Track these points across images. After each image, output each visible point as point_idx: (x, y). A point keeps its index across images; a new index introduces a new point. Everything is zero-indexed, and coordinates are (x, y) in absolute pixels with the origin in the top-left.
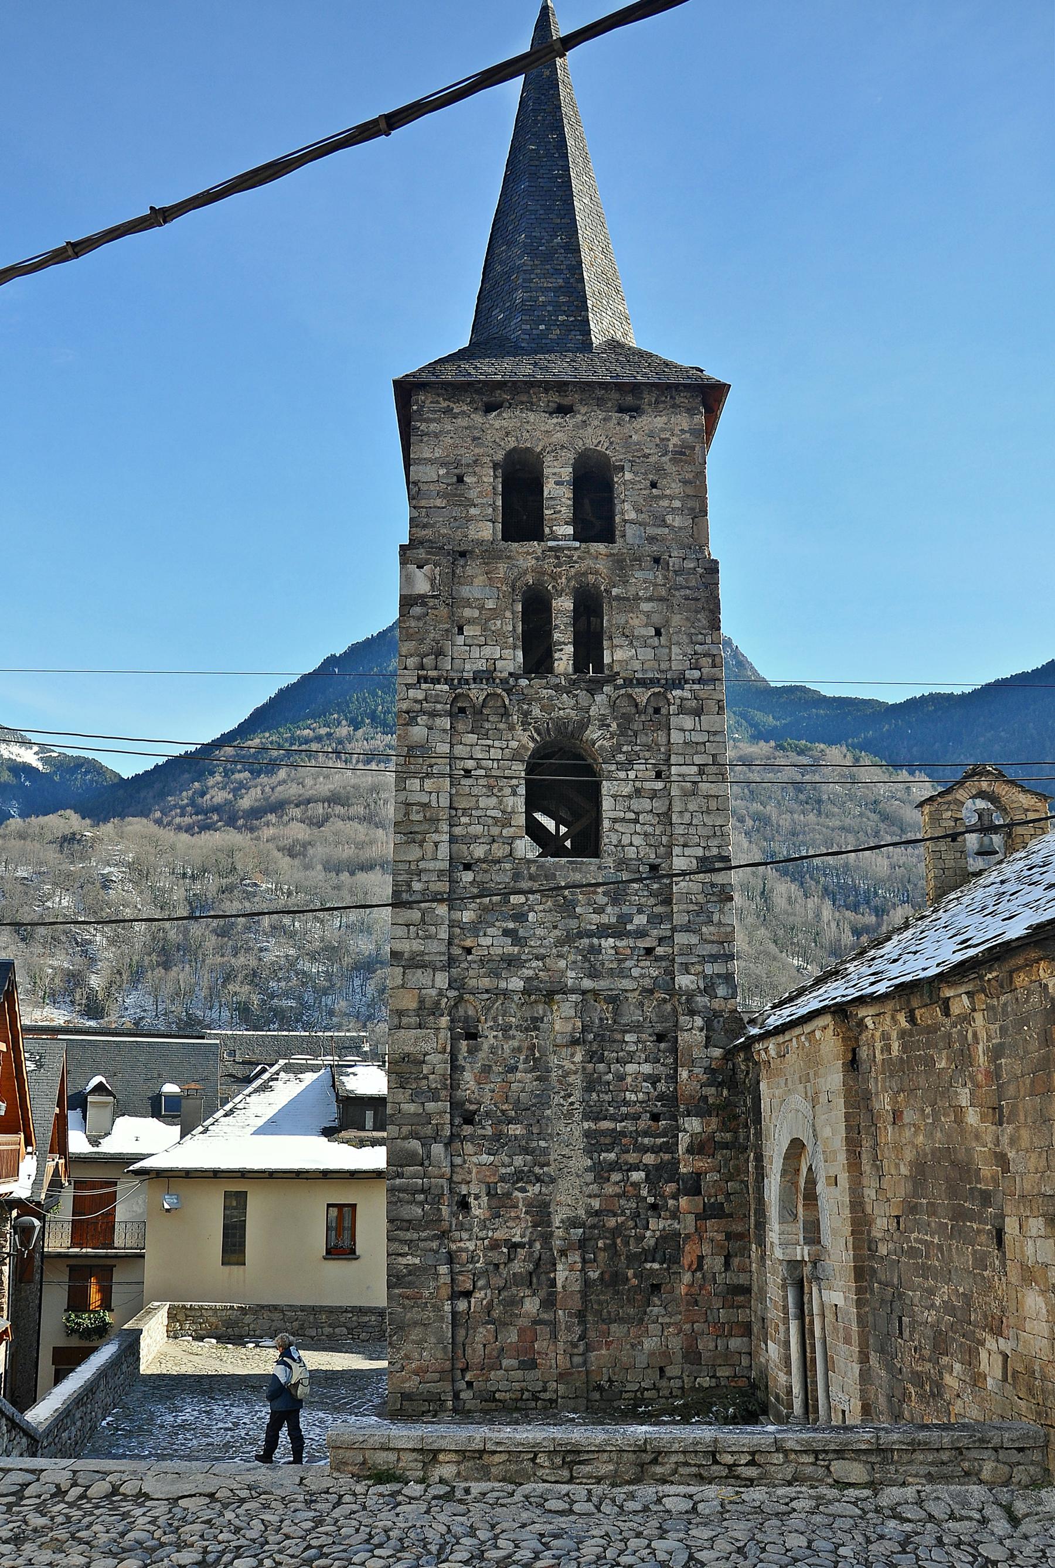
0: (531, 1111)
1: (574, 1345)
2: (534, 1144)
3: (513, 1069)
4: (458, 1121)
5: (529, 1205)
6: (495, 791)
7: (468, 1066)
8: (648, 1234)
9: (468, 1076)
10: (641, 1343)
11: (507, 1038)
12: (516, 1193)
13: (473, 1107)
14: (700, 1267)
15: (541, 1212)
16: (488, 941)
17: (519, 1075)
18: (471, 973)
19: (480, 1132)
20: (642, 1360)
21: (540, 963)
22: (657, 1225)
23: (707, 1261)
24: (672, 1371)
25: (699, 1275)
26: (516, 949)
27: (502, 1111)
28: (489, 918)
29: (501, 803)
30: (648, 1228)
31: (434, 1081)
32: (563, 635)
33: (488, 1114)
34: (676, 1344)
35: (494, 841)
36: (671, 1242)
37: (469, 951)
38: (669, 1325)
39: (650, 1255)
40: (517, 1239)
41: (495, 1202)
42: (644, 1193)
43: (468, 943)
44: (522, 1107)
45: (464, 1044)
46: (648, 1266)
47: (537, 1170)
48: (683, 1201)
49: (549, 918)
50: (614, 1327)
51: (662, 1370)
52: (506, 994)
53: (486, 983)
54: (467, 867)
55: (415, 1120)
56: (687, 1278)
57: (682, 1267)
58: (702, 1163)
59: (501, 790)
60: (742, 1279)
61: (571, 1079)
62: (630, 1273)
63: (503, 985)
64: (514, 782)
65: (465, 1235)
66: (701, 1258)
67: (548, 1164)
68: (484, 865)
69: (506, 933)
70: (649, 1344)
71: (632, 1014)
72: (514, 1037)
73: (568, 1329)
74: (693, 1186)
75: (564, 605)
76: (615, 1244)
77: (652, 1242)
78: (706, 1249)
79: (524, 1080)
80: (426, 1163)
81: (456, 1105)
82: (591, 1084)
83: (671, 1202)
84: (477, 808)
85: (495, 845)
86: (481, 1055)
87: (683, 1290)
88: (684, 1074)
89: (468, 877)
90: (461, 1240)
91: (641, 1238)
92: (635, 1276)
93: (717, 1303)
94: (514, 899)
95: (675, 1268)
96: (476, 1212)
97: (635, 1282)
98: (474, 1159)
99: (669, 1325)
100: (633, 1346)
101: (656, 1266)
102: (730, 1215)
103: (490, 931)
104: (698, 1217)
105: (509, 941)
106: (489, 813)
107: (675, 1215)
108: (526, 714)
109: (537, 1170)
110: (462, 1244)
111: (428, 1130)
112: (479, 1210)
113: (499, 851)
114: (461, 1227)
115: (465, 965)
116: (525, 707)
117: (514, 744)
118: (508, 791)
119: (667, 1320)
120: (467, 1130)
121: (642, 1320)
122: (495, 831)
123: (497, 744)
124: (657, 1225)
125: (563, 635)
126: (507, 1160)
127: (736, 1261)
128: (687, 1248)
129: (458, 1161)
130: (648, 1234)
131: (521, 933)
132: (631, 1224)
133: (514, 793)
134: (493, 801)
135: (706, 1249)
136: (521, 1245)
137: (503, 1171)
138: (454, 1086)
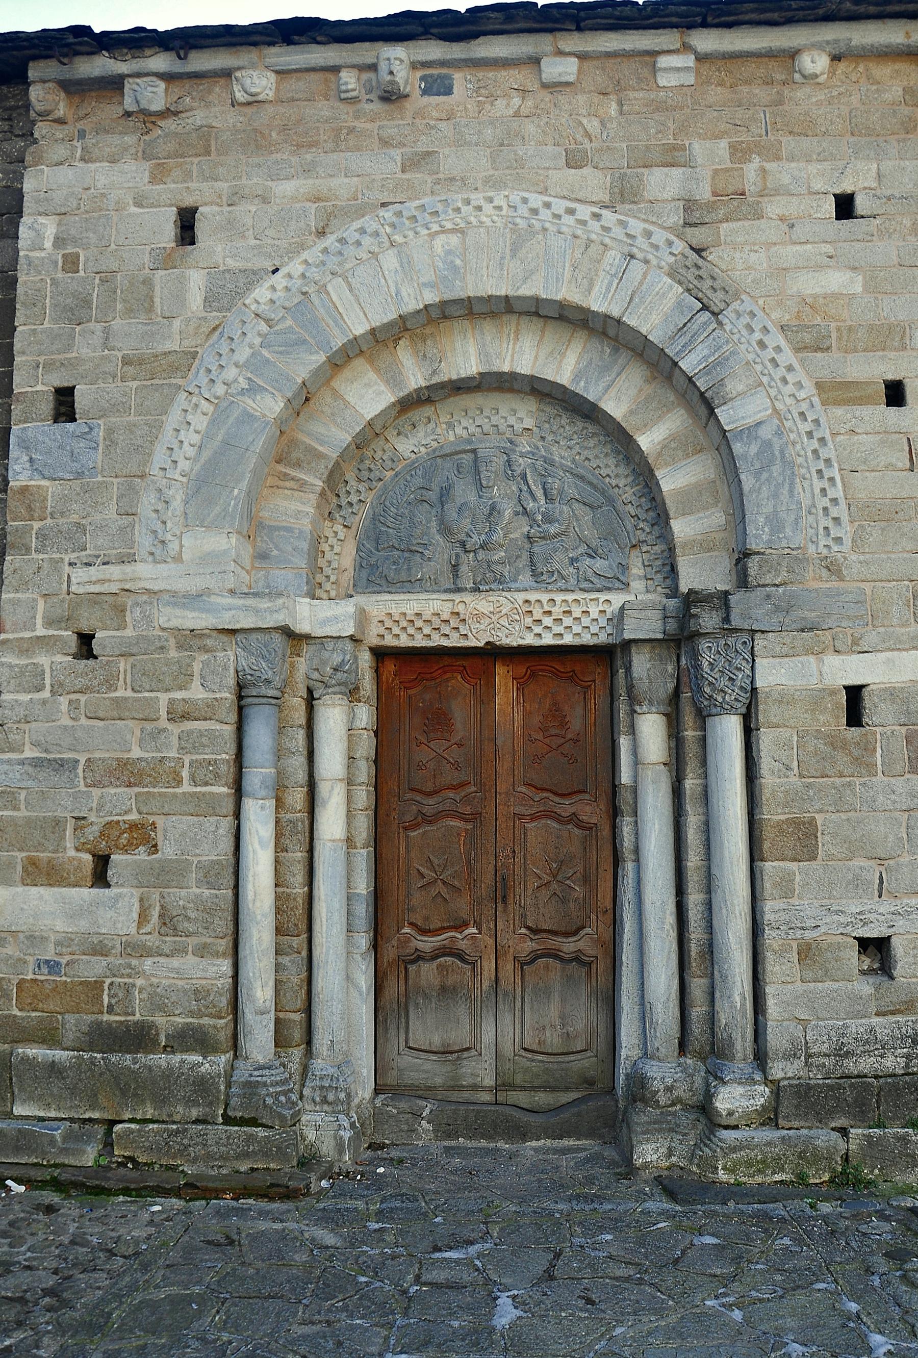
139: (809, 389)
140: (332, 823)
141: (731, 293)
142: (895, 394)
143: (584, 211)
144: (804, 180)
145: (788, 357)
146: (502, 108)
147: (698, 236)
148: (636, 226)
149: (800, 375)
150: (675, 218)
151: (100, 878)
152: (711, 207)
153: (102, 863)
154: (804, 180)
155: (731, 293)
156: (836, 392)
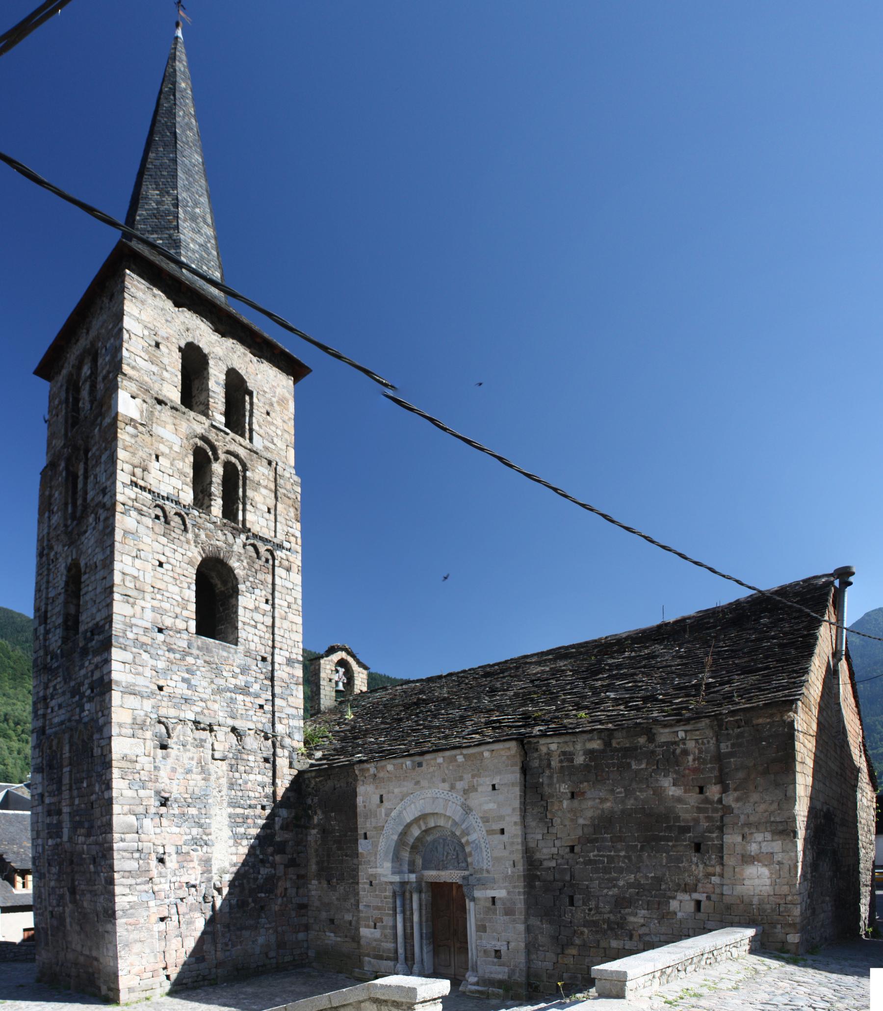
0: (199, 799)
1: (227, 945)
2: (203, 821)
3: (189, 771)
4: (158, 803)
5: (201, 860)
6: (178, 582)
7: (162, 767)
8: (260, 876)
9: (163, 774)
10: (256, 940)
11: (186, 751)
12: (192, 852)
13: (166, 795)
14: (285, 895)
15: (207, 863)
16: (172, 684)
17: (194, 776)
18: (164, 704)
19: (171, 812)
20: (258, 950)
21: (203, 704)
22: (264, 871)
23: (289, 891)
24: (272, 954)
25: (285, 899)
26: (190, 692)
27: (185, 799)
28: (174, 668)
29: (181, 591)
30: (259, 873)
31: (144, 776)
32: (216, 489)
33: (176, 800)
34: (273, 939)
35: (177, 617)
36: (271, 880)
37: (161, 688)
38: (269, 928)
39: (260, 889)
40: (193, 882)
41: (181, 858)
42: (258, 852)
43: (161, 683)
44: (195, 796)
45: (160, 752)
46: (259, 895)
47: (205, 837)
48: (278, 858)
49: (208, 675)
50: (244, 932)
51: (266, 954)
52: (182, 721)
53: (172, 712)
54: (160, 630)
55: (132, 802)
56: (280, 901)
57: (276, 895)
58: (287, 836)
59: (181, 582)
60: (305, 901)
61: (221, 781)
62: (250, 900)
63: (182, 716)
64: (189, 580)
65: (163, 880)
66: (286, 889)
67: (210, 834)
68: (171, 633)
69: (184, 680)
70: (261, 940)
71: (252, 742)
72: (189, 751)
73: (223, 935)
74: (281, 849)
75: (218, 469)
76: (242, 884)
77: (262, 881)
78: (288, 885)
79: (196, 779)
80: (140, 831)
81: (158, 793)
82: (231, 786)
83: (271, 858)
84: (167, 591)
85: (177, 621)
86: (170, 761)
87: (277, 908)
88: (278, 781)
89: (160, 637)
90: (161, 883)
91: (256, 879)
92: (253, 901)
93: (293, 914)
94: (190, 660)
95: (272, 896)
96: (168, 864)
97: (253, 905)
98: (168, 829)
99: (269, 928)
100: (253, 942)
101: (263, 895)
102: (299, 865)
103: (175, 677)
104: (286, 866)
105: (186, 685)
106: (174, 597)
107: (273, 865)
108: (197, 536)
109: (205, 837)
110: (161, 886)
111: (141, 809)
112: (172, 862)
113: (181, 625)
114: (161, 875)
115: (159, 697)
116: (197, 531)
117: (189, 554)
118: (185, 585)
119: (268, 926)
120: (163, 810)
121: (257, 927)
122: (178, 610)
123: (179, 549)
124: (264, 871)
125: (216, 489)
126: (188, 831)
127: (301, 891)
128: (280, 884)
129: (158, 830)
130: (260, 876)
131: (193, 682)
132: (251, 871)
133: (189, 588)
134: (176, 589)
135: (288, 885)
136: (194, 886)
137: (186, 837)
138: (157, 781)
139: (484, 832)
140: (416, 918)
141: (471, 810)
142: (502, 831)
143: (445, 792)
144: (486, 782)
145: (481, 825)
146: (431, 770)
147: (465, 796)
148: (454, 795)
149: (483, 829)
150: (462, 793)
151: (375, 928)
152: (468, 790)
153: (375, 925)
154: (486, 782)
155: (471, 810)
156: (490, 832)
